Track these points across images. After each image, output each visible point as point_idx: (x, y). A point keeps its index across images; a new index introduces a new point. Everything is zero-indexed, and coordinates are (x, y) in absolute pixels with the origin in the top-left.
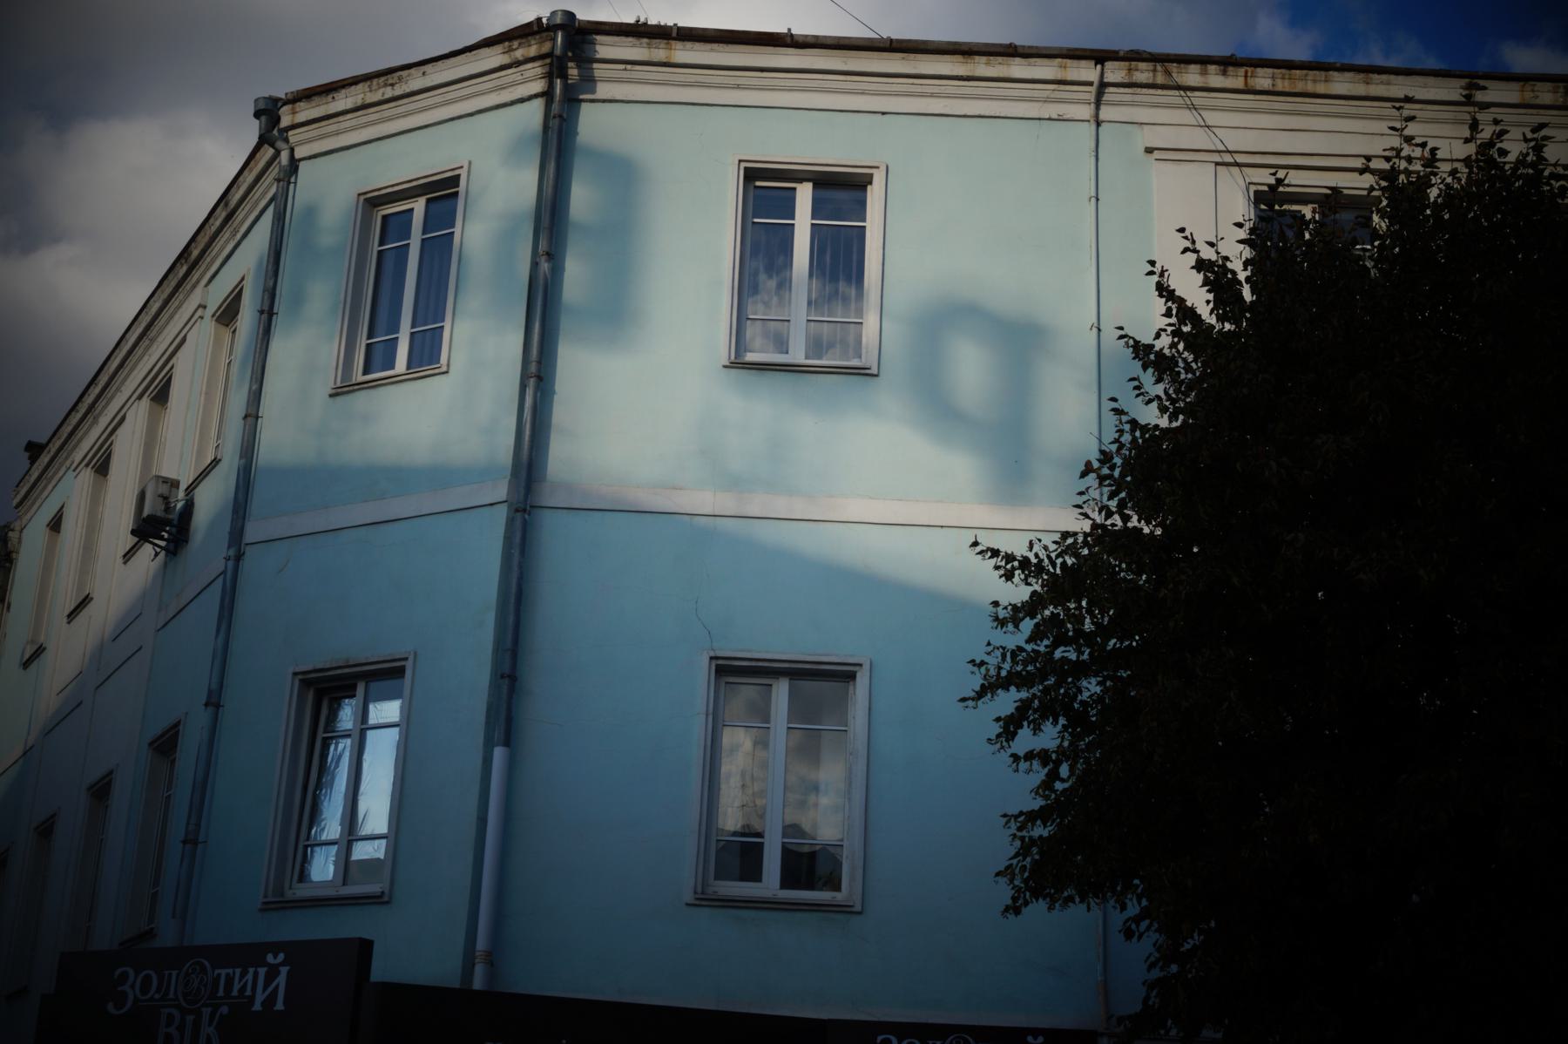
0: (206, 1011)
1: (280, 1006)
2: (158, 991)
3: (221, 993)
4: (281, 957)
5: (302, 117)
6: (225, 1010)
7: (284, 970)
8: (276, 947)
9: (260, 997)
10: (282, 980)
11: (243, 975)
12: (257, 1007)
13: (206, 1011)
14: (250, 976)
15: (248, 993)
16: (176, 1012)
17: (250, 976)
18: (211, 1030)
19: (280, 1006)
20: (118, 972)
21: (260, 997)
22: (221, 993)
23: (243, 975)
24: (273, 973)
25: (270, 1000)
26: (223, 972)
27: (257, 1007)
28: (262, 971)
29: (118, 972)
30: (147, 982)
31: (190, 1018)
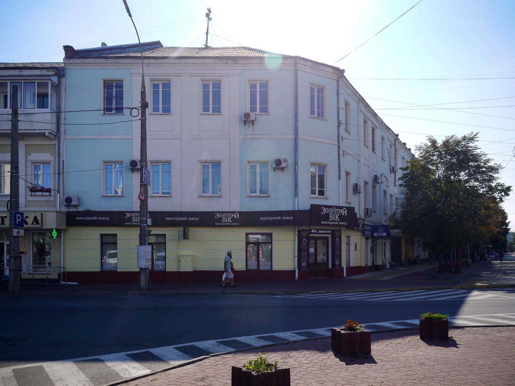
0: (336, 215)
1: (346, 215)
2: (329, 211)
3: (338, 212)
4: (345, 208)
5: (301, 63)
6: (339, 215)
7: (346, 210)
8: (345, 207)
9: (343, 213)
10: (346, 211)
11: (340, 210)
12: (343, 215)
13: (336, 215)
14: (341, 210)
15: (342, 213)
16: (332, 214)
17: (341, 210)
18: (337, 217)
19: (346, 215)
20: (322, 208)
21: (343, 213)
22: (338, 212)
23: (340, 210)
24: (344, 211)
25: (345, 214)
26: (338, 210)
27: (343, 215)
28: (343, 210)
29: (322, 208)
30: (327, 209)
31: (334, 215)
